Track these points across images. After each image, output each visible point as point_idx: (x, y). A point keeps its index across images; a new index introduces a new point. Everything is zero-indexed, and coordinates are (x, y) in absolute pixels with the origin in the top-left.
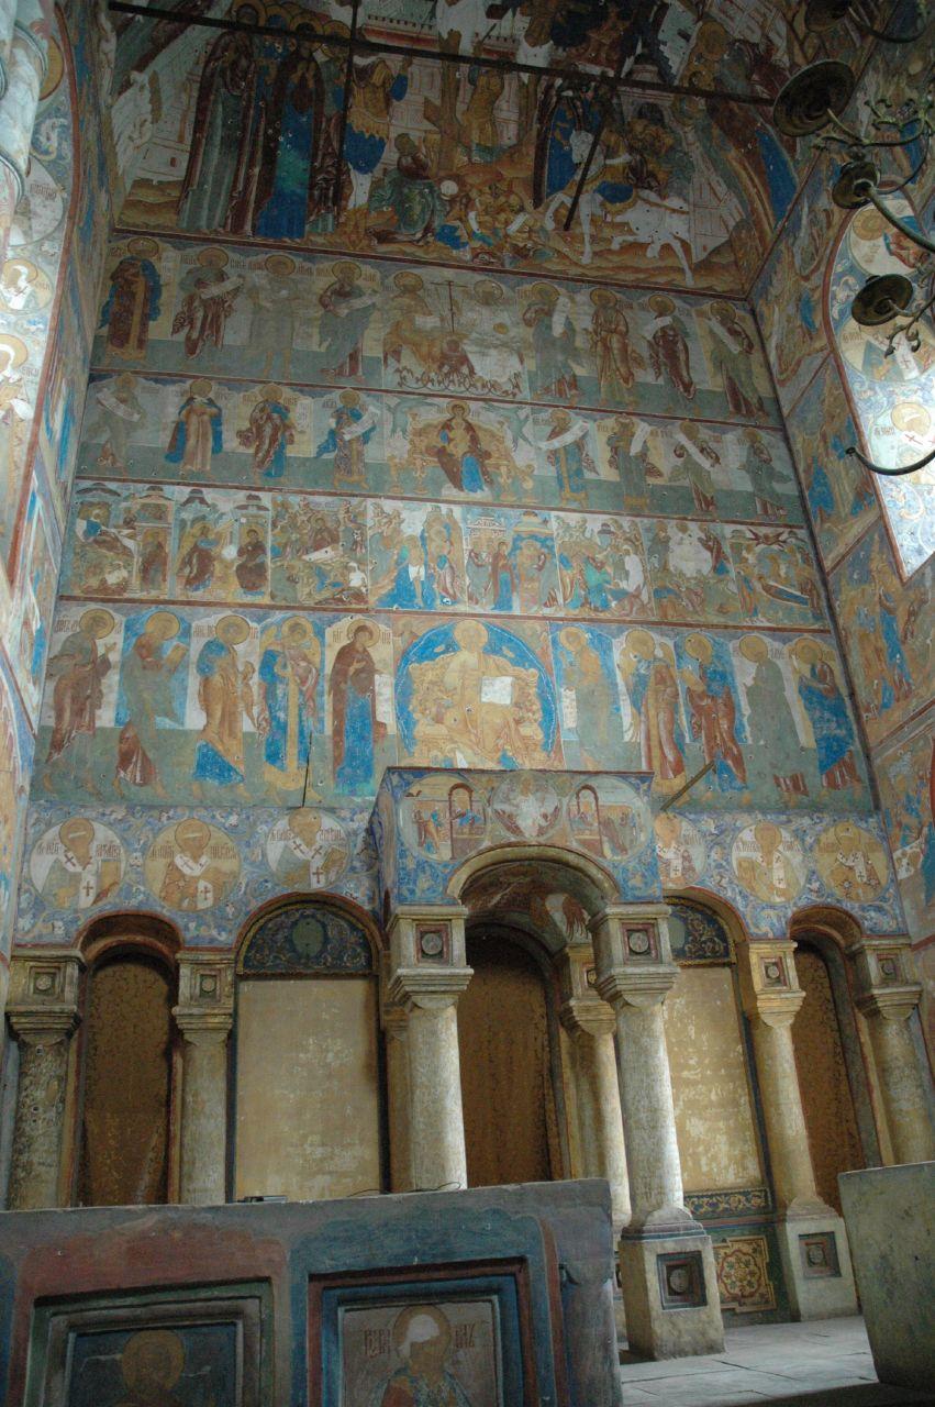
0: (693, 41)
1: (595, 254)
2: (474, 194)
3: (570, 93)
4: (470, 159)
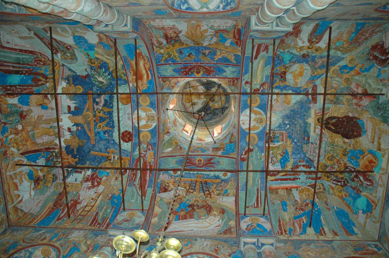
0: (76, 183)
1: (11, 176)
2: (20, 135)
3: (54, 154)
4: (29, 131)
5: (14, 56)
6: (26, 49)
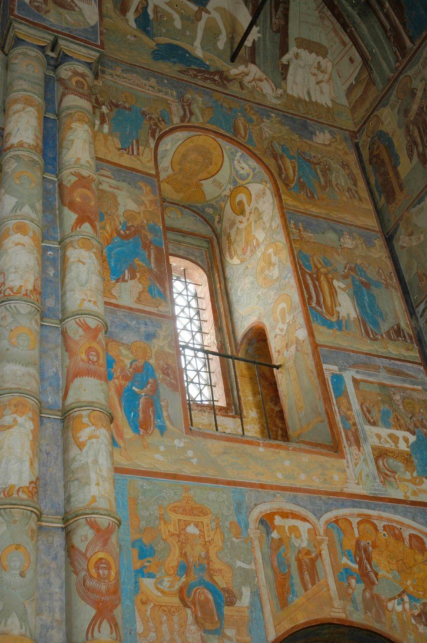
5: (364, 27)
6: (335, 21)
